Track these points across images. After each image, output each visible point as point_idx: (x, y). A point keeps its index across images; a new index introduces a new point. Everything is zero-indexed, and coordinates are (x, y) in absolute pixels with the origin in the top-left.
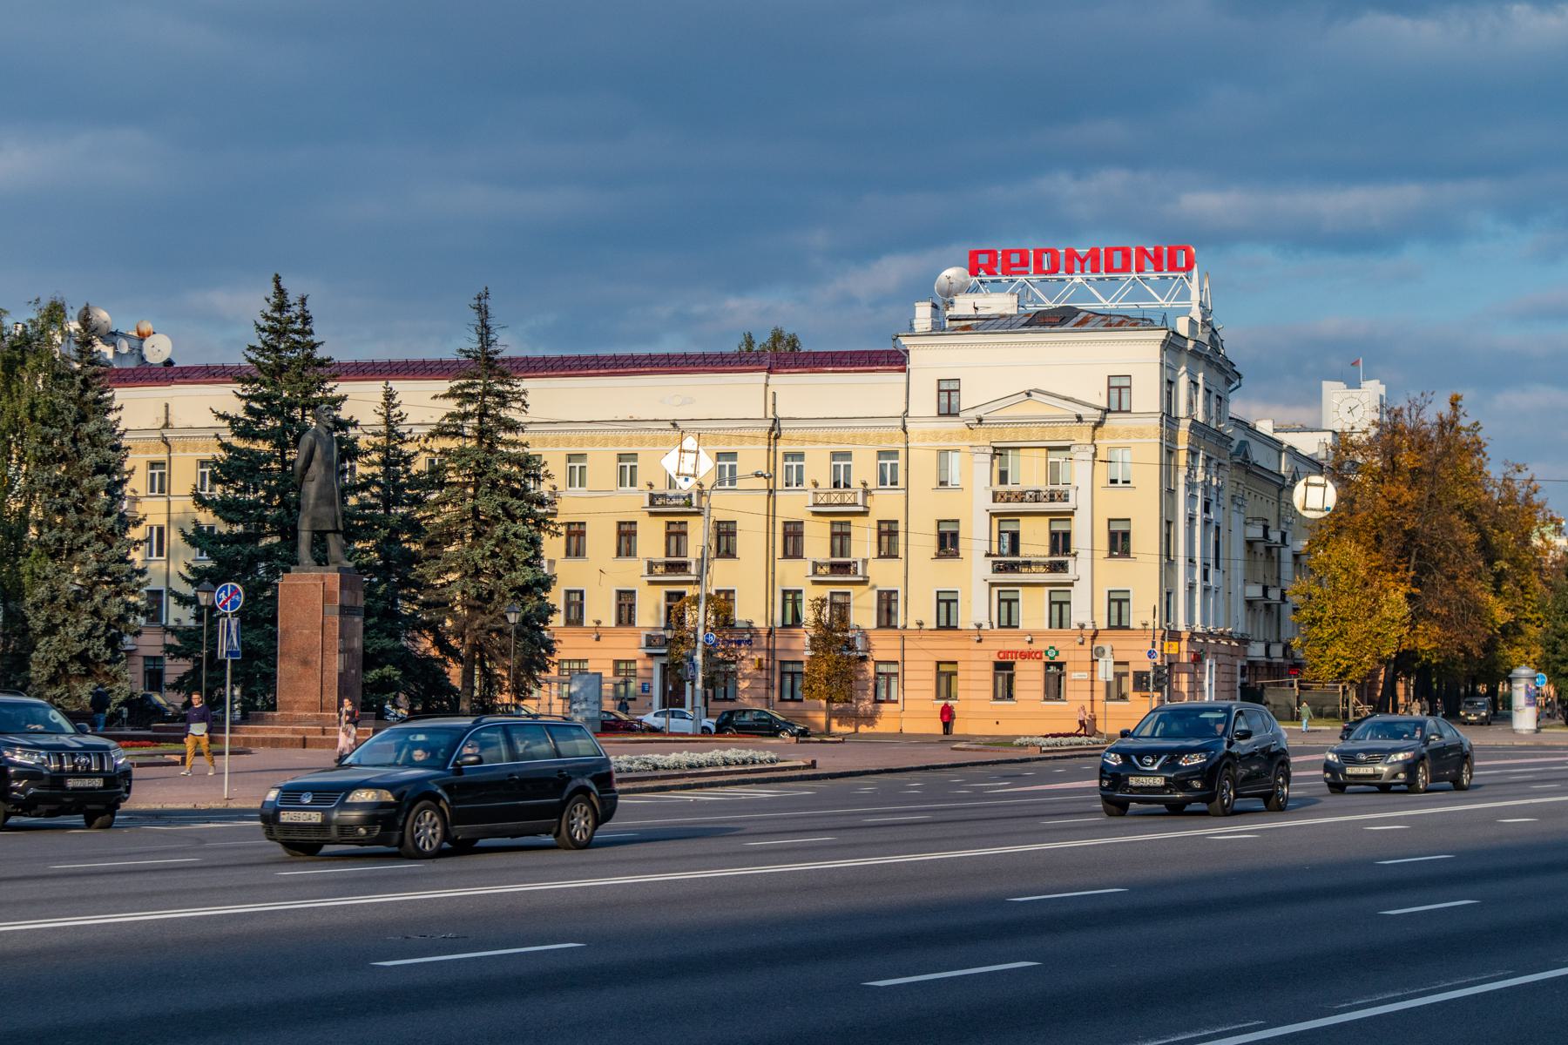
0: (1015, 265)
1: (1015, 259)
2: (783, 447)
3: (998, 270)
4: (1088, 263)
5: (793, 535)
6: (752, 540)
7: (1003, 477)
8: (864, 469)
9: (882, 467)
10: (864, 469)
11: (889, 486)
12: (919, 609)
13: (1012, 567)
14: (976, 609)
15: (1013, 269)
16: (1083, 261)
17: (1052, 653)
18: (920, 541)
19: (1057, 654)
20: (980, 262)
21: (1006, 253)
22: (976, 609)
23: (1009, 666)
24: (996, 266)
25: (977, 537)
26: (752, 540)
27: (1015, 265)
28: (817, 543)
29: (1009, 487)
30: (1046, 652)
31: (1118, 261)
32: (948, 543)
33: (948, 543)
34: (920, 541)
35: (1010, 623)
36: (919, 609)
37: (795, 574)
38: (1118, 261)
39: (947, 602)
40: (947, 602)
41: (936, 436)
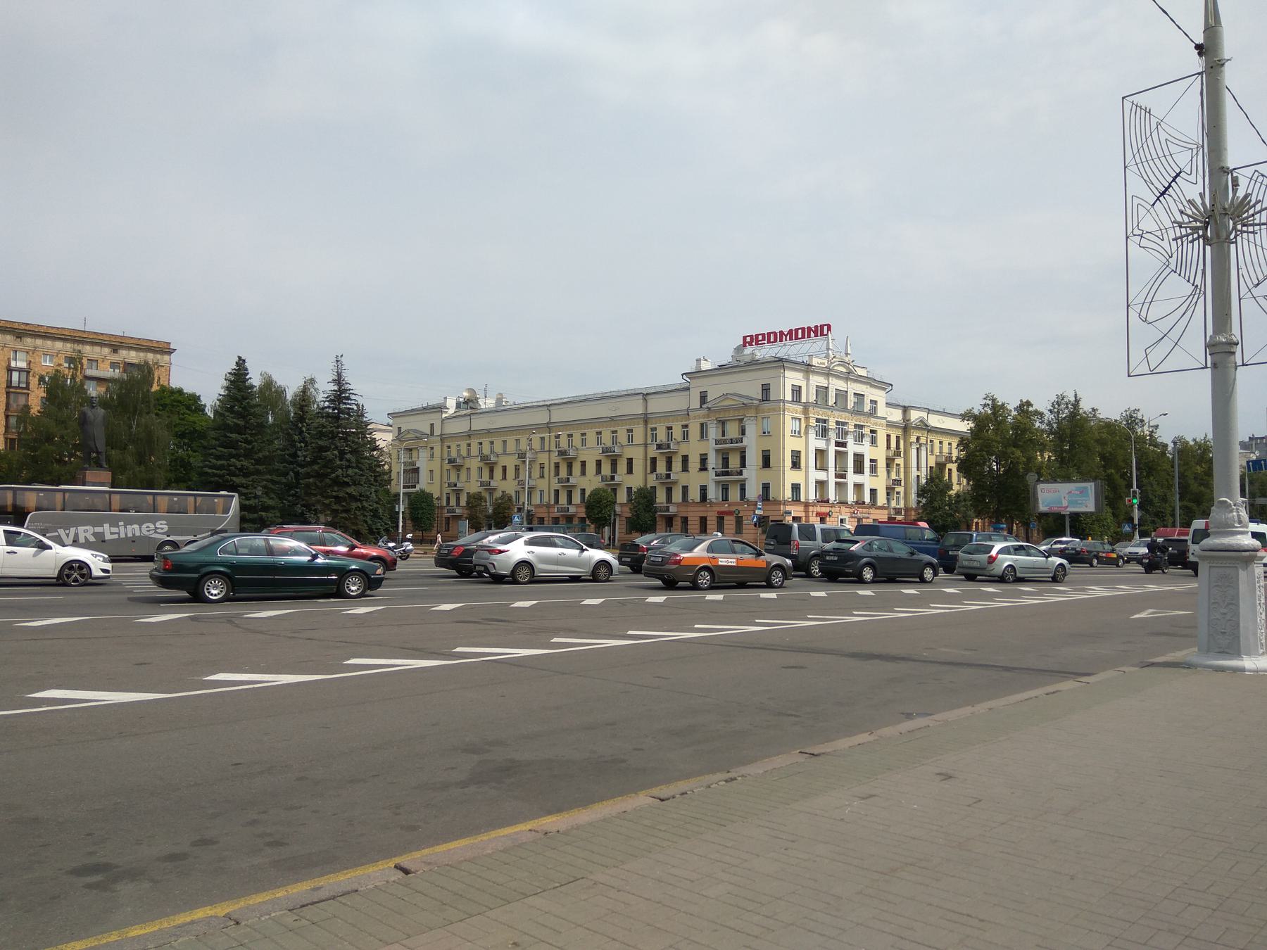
0: (760, 341)
1: (760, 337)
2: (650, 426)
4: (788, 337)
5: (654, 460)
8: (677, 433)
10: (677, 433)
13: (727, 474)
14: (713, 494)
16: (786, 336)
18: (694, 463)
19: (739, 512)
23: (722, 518)
25: (713, 461)
26: (638, 466)
27: (760, 341)
28: (661, 468)
34: (694, 463)
35: (726, 498)
39: (704, 490)
40: (704, 490)
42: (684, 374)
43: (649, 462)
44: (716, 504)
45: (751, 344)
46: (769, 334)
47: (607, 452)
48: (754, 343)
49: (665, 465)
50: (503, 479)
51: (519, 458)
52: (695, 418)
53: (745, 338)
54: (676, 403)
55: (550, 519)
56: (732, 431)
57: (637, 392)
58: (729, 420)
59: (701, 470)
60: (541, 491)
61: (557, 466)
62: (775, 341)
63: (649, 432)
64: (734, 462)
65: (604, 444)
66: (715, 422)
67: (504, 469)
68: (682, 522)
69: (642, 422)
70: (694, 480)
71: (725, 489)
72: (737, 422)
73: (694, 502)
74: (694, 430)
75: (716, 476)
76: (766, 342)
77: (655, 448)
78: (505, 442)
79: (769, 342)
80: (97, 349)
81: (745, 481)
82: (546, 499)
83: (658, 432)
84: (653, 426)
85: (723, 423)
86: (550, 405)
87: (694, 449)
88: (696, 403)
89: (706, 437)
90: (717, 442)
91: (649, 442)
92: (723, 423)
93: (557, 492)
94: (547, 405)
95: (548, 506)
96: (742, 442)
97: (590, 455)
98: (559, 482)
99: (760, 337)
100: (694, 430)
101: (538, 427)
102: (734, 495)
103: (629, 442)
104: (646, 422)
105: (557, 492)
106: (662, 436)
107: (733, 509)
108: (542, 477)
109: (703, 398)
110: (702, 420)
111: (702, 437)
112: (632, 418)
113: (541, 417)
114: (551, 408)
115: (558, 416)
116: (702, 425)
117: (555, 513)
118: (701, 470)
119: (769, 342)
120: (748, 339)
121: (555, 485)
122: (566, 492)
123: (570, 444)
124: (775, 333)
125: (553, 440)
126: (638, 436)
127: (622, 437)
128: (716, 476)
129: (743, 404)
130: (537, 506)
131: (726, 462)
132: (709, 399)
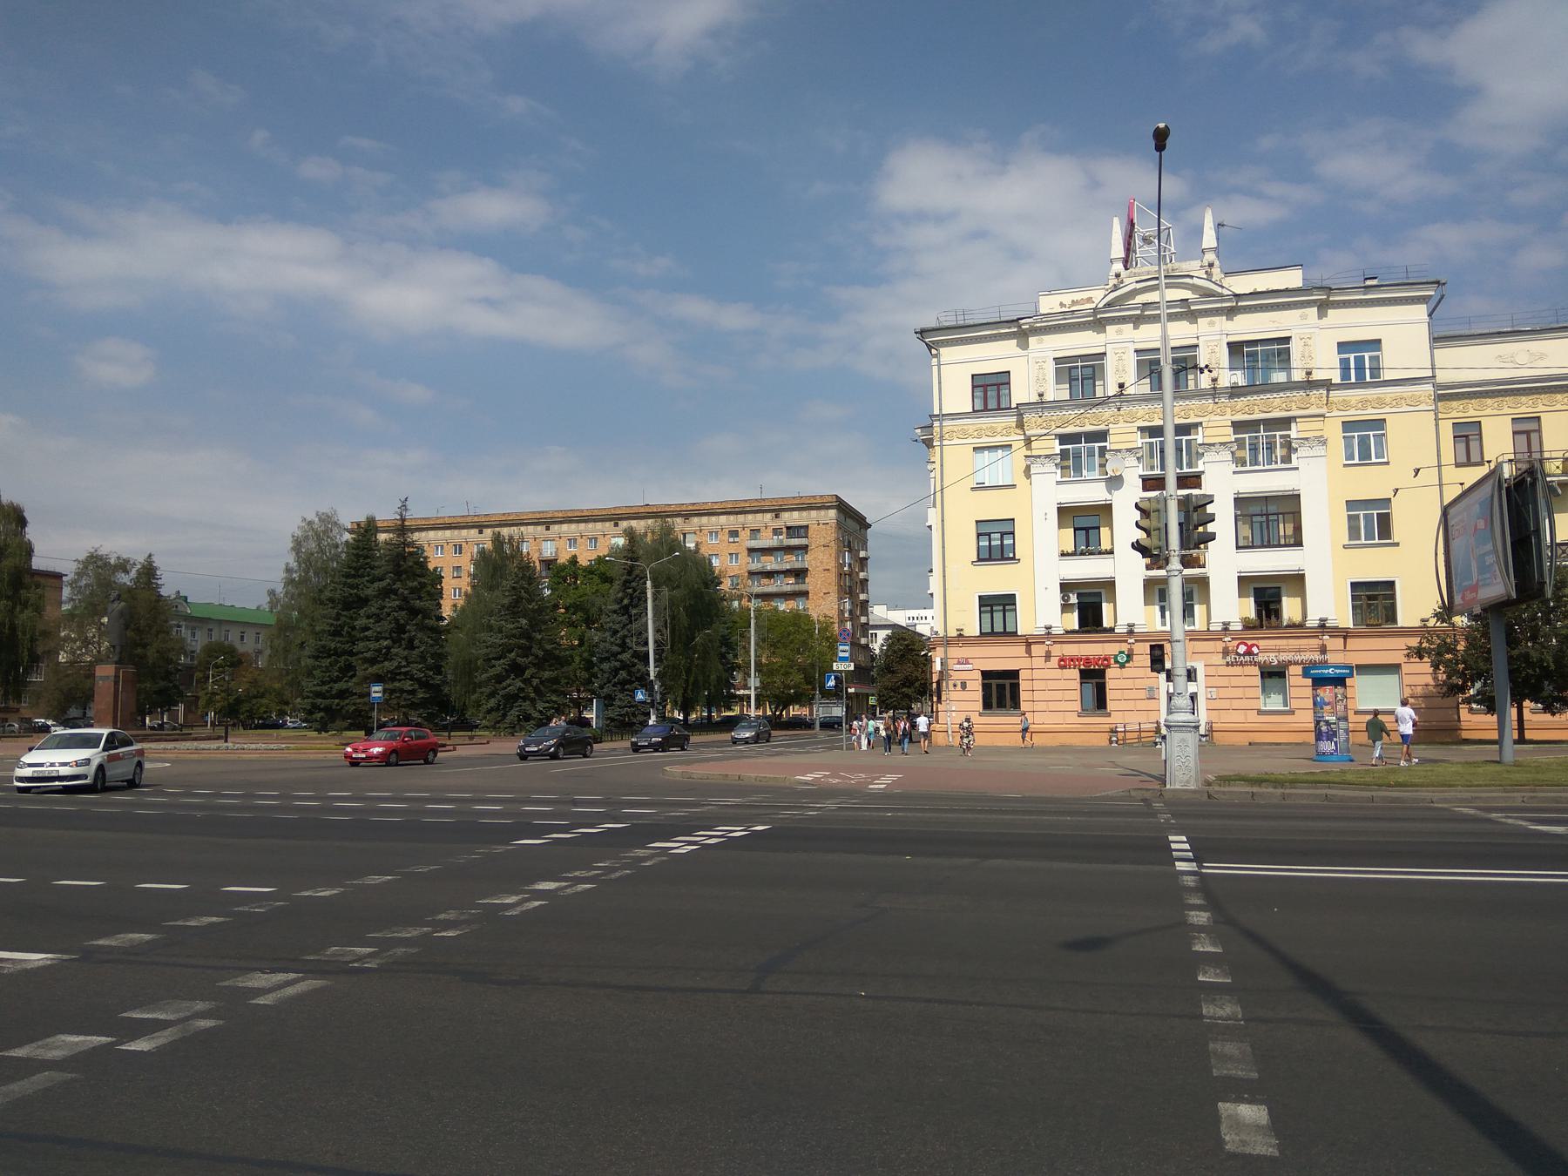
80: (759, 516)
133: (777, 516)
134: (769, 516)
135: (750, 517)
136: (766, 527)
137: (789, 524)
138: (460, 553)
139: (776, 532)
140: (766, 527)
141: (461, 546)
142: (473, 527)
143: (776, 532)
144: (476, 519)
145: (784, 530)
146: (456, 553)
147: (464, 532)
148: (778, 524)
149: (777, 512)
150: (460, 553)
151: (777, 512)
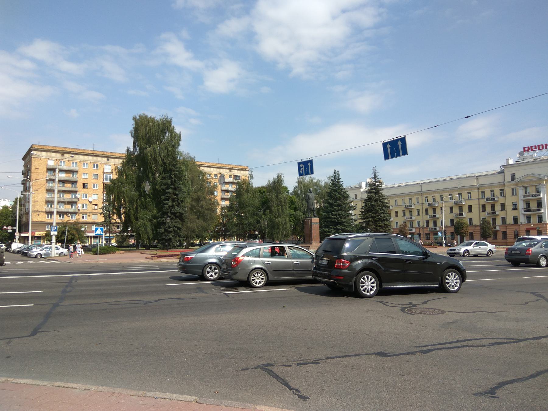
1: (533, 148)
2: (480, 190)
3: (530, 150)
5: (484, 207)
6: (475, 209)
7: (526, 193)
8: (497, 192)
9: (501, 192)
10: (497, 192)
11: (502, 196)
12: (510, 220)
14: (522, 220)
15: (533, 150)
17: (538, 228)
18: (509, 207)
19: (539, 228)
20: (526, 149)
21: (531, 147)
22: (522, 220)
24: (529, 150)
25: (521, 206)
26: (475, 209)
29: (527, 194)
30: (537, 228)
31: (541, 147)
32: (515, 207)
33: (515, 207)
36: (510, 220)
37: (484, 215)
38: (541, 147)
39: (516, 220)
40: (516, 220)
41: (511, 185)
42: (502, 166)
43: (481, 206)
44: (525, 225)
45: (528, 150)
46: (539, 146)
47: (457, 203)
48: (530, 150)
49: (491, 207)
50: (396, 217)
51: (406, 207)
52: (508, 185)
53: (524, 148)
54: (499, 179)
55: (425, 234)
56: (531, 191)
57: (473, 175)
58: (529, 186)
59: (513, 209)
60: (418, 221)
61: (427, 210)
62: (543, 148)
63: (480, 193)
64: (534, 205)
65: (455, 200)
66: (522, 187)
67: (397, 212)
68: (502, 234)
69: (477, 189)
70: (510, 215)
71: (529, 218)
72: (535, 187)
73: (510, 224)
74: (508, 191)
75: (524, 212)
76: (537, 149)
77: (486, 201)
78: (396, 201)
79: (539, 149)
81: (542, 214)
82: (421, 225)
83: (485, 193)
84: (483, 190)
85: (526, 188)
86: (422, 183)
87: (509, 201)
88: (508, 178)
89: (516, 194)
90: (525, 196)
91: (481, 197)
92: (526, 188)
93: (427, 222)
94: (420, 184)
95: (423, 228)
96: (539, 196)
97: (445, 205)
98: (429, 217)
99: (533, 148)
100: (508, 191)
101: (414, 194)
102: (534, 220)
103: (469, 198)
104: (478, 189)
105: (427, 222)
106: (488, 195)
107: (536, 227)
108: (418, 215)
109: (513, 177)
110: (513, 187)
111: (513, 194)
112: (472, 187)
113: (418, 189)
114: (422, 185)
115: (425, 188)
116: (513, 189)
117: (428, 230)
118: (513, 209)
119: (539, 149)
120: (526, 149)
121: (426, 218)
122: (433, 221)
123: (434, 200)
124: (542, 145)
125: (424, 198)
126: (475, 194)
127: (465, 195)
128: (524, 212)
129: (540, 178)
130: (416, 228)
131: (528, 205)
132: (517, 177)
133: (230, 171)
134: (228, 171)
135: (221, 170)
136: (227, 174)
137: (235, 175)
138: (97, 168)
139: (230, 177)
140: (227, 174)
141: (97, 165)
142: (104, 157)
143: (230, 177)
144: (105, 153)
145: (233, 176)
146: (94, 167)
147: (99, 159)
148: (231, 174)
149: (230, 170)
150: (97, 168)
151: (230, 170)
